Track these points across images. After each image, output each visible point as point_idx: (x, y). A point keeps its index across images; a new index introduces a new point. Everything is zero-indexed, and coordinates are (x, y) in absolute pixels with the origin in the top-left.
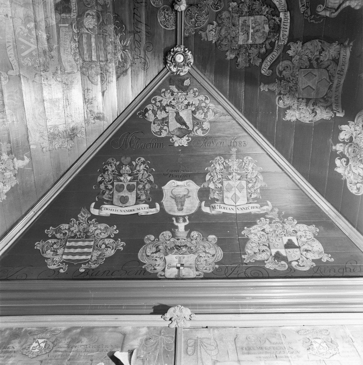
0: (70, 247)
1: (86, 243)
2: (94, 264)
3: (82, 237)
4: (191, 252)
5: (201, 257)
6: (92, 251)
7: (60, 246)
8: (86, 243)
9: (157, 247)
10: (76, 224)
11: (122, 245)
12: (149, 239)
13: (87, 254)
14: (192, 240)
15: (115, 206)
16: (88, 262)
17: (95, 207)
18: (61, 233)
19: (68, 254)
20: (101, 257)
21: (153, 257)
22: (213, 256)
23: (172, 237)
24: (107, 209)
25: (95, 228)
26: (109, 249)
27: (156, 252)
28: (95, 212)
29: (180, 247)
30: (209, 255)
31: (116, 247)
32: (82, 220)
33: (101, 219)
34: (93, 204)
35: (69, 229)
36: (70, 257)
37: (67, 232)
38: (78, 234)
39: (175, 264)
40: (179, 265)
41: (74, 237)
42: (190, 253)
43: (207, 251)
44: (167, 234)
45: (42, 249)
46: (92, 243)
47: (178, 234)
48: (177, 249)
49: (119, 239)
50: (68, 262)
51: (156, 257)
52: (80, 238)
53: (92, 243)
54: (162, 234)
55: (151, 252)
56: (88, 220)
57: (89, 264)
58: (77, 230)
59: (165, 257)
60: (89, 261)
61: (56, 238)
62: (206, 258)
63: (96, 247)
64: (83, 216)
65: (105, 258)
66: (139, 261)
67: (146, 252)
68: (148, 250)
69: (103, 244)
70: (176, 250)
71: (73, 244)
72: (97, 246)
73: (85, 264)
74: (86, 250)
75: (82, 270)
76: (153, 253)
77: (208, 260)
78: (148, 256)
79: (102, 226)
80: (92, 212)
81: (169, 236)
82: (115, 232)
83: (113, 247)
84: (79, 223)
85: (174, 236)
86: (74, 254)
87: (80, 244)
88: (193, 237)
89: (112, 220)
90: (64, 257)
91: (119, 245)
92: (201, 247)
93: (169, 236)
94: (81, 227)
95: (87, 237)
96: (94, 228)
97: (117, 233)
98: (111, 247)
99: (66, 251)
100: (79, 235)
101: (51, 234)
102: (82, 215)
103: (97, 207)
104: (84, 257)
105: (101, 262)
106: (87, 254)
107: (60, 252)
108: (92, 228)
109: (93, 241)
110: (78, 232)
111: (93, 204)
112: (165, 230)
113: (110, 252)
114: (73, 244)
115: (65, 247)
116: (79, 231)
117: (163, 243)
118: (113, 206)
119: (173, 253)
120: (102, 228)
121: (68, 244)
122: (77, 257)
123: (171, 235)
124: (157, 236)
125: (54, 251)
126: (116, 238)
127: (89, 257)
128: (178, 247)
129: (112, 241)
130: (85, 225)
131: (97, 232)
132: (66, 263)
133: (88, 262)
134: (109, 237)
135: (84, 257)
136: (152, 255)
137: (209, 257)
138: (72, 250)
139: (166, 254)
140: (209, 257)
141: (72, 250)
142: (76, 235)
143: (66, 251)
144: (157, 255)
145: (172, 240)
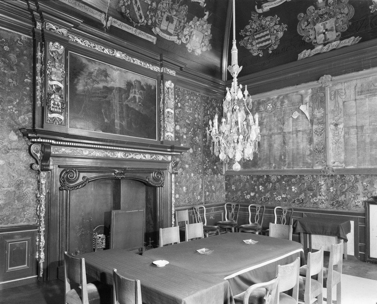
0: (257, 39)
1: (265, 33)
2: (275, 46)
4: (331, 17)
5: (338, 18)
7: (252, 39)
8: (265, 33)
9: (307, 21)
10: (253, 23)
12: (300, 17)
13: (268, 40)
14: (330, 6)
15: (270, 2)
16: (271, 46)
17: (258, 8)
18: (248, 31)
19: (258, 43)
20: (277, 40)
21: (307, 29)
22: (347, 14)
23: (315, 10)
24: (266, 6)
25: (265, 21)
26: (279, 32)
27: (308, 25)
28: (260, 11)
29: (322, 15)
30: (344, 15)
31: (283, 29)
32: (255, 19)
33: (266, 14)
34: (256, 6)
35: (251, 27)
36: (261, 45)
38: (257, 29)
39: (321, 31)
40: (324, 31)
41: (256, 32)
42: (330, 18)
43: (343, 12)
44: (311, 8)
45: (244, 45)
46: (268, 32)
47: (319, 6)
48: (321, 17)
49: (282, 24)
50: (260, 49)
51: (309, 29)
52: (260, 31)
53: (268, 32)
54: (307, 10)
55: (305, 25)
56: (258, 18)
58: (256, 27)
59: (314, 27)
61: (247, 36)
62: (342, 19)
63: (271, 34)
64: (254, 17)
67: (301, 27)
68: (302, 24)
69: (274, 30)
70: (320, 19)
71: (258, 36)
72: (271, 33)
73: (270, 47)
74: (267, 37)
75: (270, 52)
77: (343, 20)
78: (303, 30)
79: (268, 18)
80: (258, 12)
81: (313, 10)
82: (278, 20)
84: (255, 22)
85: (317, 8)
86: (262, 42)
87: (262, 34)
88: (330, 3)
89: (272, 12)
90: (258, 46)
91: (284, 27)
92: (337, 10)
93: (313, 10)
94: (257, 24)
95: (263, 29)
96: (265, 22)
97: (279, 19)
99: (257, 41)
100: (259, 29)
102: (253, 16)
103: (260, 7)
104: (267, 43)
105: (278, 43)
106: (268, 40)
107: (254, 43)
108: (263, 22)
109: (267, 30)
110: (257, 27)
111: (256, 6)
112: (309, 6)
113: (281, 34)
114: (258, 36)
115: (254, 39)
116: (257, 27)
117: (310, 17)
118: (269, 3)
119: (319, 22)
120: (269, 20)
121: (255, 37)
122: (264, 44)
123: (314, 8)
124: (305, 13)
125: (251, 44)
126: (280, 24)
127: (270, 41)
128: (321, 16)
129: (278, 26)
130: (259, 22)
131: (268, 23)
132: (261, 50)
133: (271, 46)
134: (276, 24)
135: (267, 43)
136: (306, 28)
137: (344, 17)
138: (260, 40)
139: (315, 24)
140: (344, 17)
141: (260, 40)
142: (257, 30)
143: (257, 41)
145: (316, 12)
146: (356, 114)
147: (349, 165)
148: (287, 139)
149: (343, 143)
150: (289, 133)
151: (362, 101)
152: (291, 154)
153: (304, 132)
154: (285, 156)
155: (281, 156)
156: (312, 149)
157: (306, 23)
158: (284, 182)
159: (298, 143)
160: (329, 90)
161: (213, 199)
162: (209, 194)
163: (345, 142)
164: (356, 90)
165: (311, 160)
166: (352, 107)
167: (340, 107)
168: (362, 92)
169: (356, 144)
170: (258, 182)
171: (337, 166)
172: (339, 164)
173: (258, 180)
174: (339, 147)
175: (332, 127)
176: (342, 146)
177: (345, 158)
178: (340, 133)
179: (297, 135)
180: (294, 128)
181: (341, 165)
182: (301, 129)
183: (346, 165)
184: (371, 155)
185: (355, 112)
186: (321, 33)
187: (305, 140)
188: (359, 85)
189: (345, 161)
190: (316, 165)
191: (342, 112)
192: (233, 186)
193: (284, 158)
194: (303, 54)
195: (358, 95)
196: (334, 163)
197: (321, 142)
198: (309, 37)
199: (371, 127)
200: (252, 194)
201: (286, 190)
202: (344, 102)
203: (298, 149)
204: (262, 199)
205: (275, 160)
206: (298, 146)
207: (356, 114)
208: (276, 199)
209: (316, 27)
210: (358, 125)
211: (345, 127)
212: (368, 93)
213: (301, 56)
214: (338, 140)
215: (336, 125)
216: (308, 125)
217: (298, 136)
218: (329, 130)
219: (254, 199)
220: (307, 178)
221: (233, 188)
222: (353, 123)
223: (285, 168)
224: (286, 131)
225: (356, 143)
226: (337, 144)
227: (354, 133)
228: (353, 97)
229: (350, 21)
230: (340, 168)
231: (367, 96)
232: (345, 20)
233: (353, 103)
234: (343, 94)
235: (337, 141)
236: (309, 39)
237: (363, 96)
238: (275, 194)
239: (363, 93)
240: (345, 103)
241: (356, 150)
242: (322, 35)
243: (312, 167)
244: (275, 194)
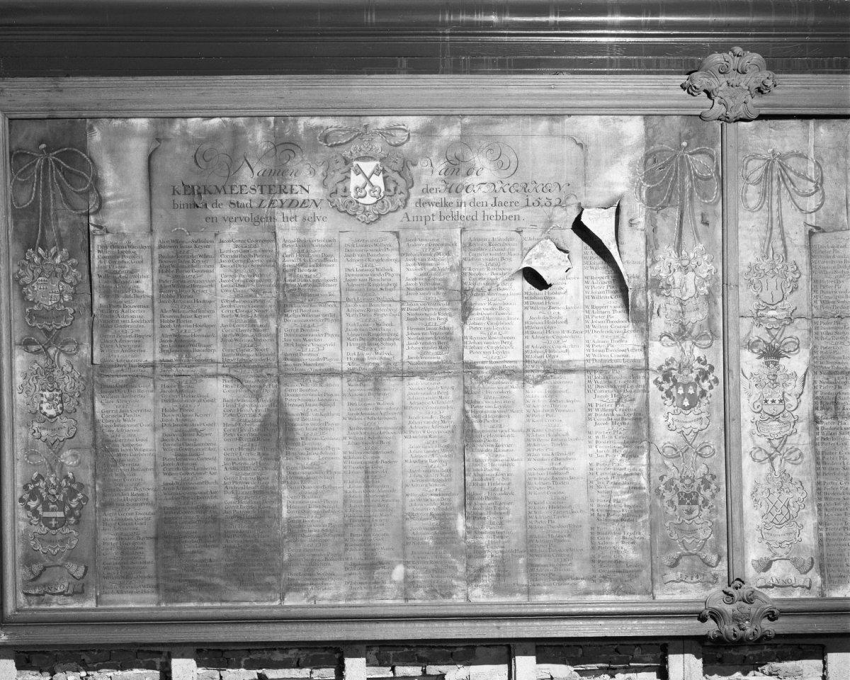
163: (816, 453)
171: (784, 585)
172: (793, 575)
178: (792, 401)
189: (821, 556)
196: (766, 566)
202: (811, 234)
214: (784, 440)
215: (772, 354)
226: (777, 461)
230: (797, 594)
234: (811, 185)
235: (776, 443)
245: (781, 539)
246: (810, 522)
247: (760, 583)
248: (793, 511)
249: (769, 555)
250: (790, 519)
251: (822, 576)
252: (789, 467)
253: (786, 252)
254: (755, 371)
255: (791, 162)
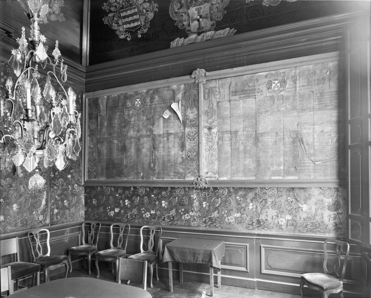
0: (124, 17)
2: (145, 29)
3: (128, 6)
5: (213, 4)
6: (139, 17)
7: (118, 18)
8: (133, 11)
9: (180, 3)
11: (156, 6)
16: (140, 28)
18: (113, 6)
20: (147, 21)
27: (181, 8)
31: (153, 9)
36: (128, 26)
37: (116, 4)
38: (124, 4)
39: (195, 17)
45: (109, 23)
46: (136, 10)
49: (152, 2)
50: (128, 30)
52: (127, 8)
53: (136, 10)
55: (177, 8)
57: (141, 29)
59: (188, 11)
60: (141, 27)
62: (217, 5)
63: (140, 13)
65: (150, 21)
66: (171, 19)
68: (175, 6)
71: (124, 14)
72: (140, 11)
73: (139, 29)
74: (135, 17)
76: (179, 9)
77: (219, 7)
78: (176, 13)
83: (151, 10)
86: (129, 23)
87: (129, 12)
90: (125, 26)
98: (150, 10)
99: (124, 21)
100: (125, 5)
101: (107, 9)
105: (148, 25)
107: (120, 22)
110: (123, 3)
113: (151, 15)
114: (124, 14)
115: (120, 17)
119: (193, 6)
121: (122, 15)
122: (132, 25)
125: (117, 23)
129: (148, 4)
132: (129, 32)
135: (136, 24)
137: (219, 3)
138: (127, 20)
139: (188, 8)
141: (127, 20)
142: (123, 6)
143: (124, 21)
144: (181, 10)
146: (230, 117)
147: (222, 176)
148: (157, 142)
149: (217, 150)
150: (160, 136)
151: (236, 103)
152: (161, 161)
153: (175, 135)
154: (154, 164)
155: (150, 164)
156: (184, 156)
157: (179, 5)
158: (153, 196)
159: (169, 148)
160: (203, 88)
161: (66, 218)
162: (59, 212)
163: (218, 149)
164: (231, 90)
165: (183, 169)
166: (227, 109)
167: (214, 108)
168: (236, 92)
169: (230, 152)
170: (123, 195)
171: (211, 177)
172: (213, 175)
173: (124, 193)
174: (212, 154)
175: (206, 131)
176: (215, 153)
177: (218, 168)
178: (214, 138)
179: (168, 139)
180: (165, 130)
181: (214, 176)
182: (172, 131)
183: (219, 176)
184: (244, 165)
185: (229, 115)
186: (195, 20)
187: (177, 145)
188: (233, 84)
189: (218, 171)
190: (189, 175)
191: (216, 113)
192: (94, 200)
193: (154, 166)
194: (176, 43)
195: (233, 96)
196: (207, 173)
197: (194, 148)
198: (182, 23)
199: (245, 133)
200: (117, 210)
201: (155, 205)
202: (218, 103)
203: (168, 155)
204: (128, 216)
205: (143, 168)
206: (169, 152)
207: (230, 117)
208: (144, 216)
209: (190, 11)
210: (232, 130)
211: (218, 131)
212: (242, 94)
213: (173, 44)
214: (212, 146)
215: (210, 129)
216: (180, 128)
217: (170, 140)
218: (203, 134)
219: (118, 216)
220: (179, 191)
221: (94, 202)
222: (227, 127)
223: (155, 179)
224: (156, 133)
225: (230, 150)
226: (211, 151)
227: (228, 139)
228: (227, 98)
229: (225, 9)
230: (213, 179)
231: (241, 97)
232: (221, 7)
233: (227, 105)
234: (218, 93)
235: (210, 147)
236: (182, 25)
237: (237, 97)
238: (143, 210)
239: (237, 94)
240: (220, 104)
241: (230, 158)
242: (196, 22)
243: (184, 178)
244: (143, 210)
245: (210, 167)
246: (216, 163)
247: (205, 177)
248: (213, 161)
249: (208, 171)
250: (213, 163)
251: (218, 175)
252: (213, 152)
253: (213, 107)
254: (207, 132)
255: (213, 89)
